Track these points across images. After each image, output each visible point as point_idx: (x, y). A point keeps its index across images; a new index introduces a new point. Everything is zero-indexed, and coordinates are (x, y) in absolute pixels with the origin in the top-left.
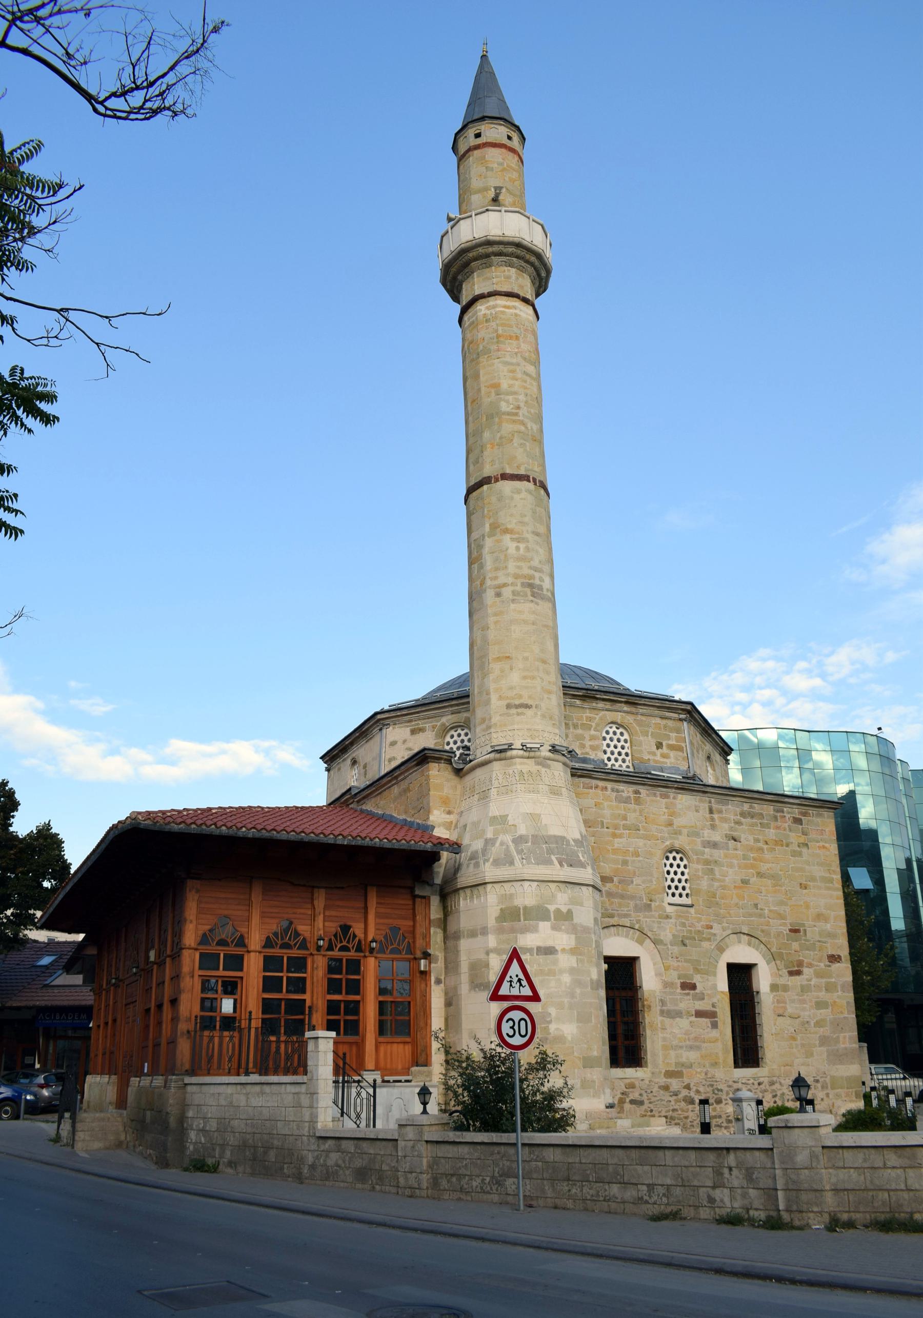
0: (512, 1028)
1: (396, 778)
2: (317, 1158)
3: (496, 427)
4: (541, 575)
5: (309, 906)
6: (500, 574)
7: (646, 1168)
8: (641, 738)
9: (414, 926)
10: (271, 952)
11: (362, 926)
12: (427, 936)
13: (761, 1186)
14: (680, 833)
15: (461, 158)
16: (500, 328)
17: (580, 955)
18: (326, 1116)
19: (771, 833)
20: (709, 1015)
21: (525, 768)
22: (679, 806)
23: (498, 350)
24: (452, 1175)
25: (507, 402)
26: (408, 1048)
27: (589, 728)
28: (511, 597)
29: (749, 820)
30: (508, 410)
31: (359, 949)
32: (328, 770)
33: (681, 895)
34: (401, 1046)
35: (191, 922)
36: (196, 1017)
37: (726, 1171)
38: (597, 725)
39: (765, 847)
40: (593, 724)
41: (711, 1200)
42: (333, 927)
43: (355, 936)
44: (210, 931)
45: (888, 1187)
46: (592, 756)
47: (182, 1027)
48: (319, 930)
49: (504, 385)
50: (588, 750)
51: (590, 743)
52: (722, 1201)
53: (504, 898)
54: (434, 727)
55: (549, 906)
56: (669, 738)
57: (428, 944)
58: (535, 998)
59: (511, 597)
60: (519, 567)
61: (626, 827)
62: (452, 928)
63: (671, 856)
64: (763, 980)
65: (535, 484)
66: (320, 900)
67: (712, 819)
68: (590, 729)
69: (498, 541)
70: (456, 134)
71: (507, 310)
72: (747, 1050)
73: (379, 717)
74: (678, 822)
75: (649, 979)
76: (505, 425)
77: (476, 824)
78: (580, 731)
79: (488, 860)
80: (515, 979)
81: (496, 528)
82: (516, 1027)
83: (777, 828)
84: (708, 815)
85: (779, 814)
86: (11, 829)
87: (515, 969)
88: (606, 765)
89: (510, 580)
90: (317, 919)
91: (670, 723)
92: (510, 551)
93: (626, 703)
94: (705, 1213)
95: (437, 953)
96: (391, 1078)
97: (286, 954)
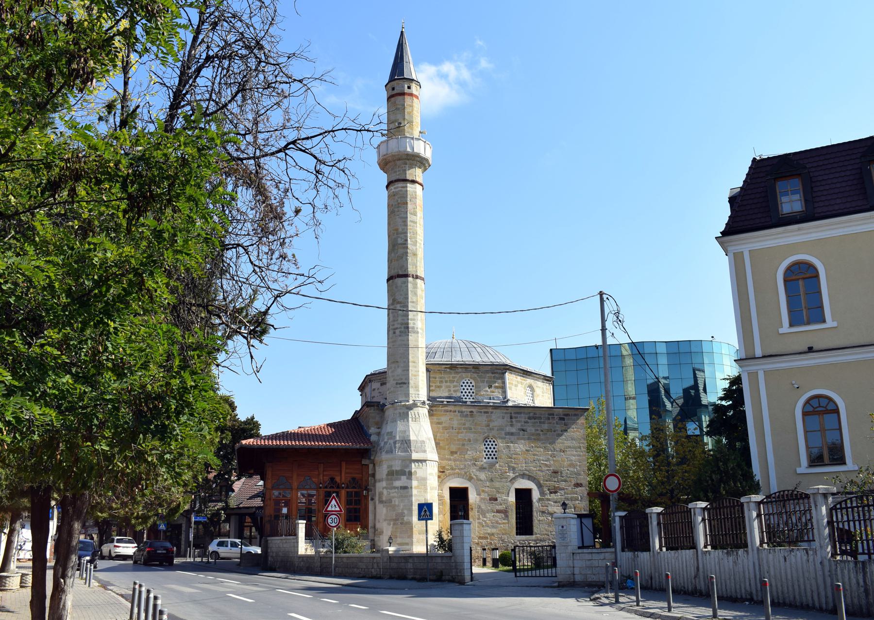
12: (367, 481)
20: (505, 512)
21: (401, 411)
49: (400, 230)
61: (464, 429)
64: (536, 495)
75: (473, 497)
91: (497, 375)
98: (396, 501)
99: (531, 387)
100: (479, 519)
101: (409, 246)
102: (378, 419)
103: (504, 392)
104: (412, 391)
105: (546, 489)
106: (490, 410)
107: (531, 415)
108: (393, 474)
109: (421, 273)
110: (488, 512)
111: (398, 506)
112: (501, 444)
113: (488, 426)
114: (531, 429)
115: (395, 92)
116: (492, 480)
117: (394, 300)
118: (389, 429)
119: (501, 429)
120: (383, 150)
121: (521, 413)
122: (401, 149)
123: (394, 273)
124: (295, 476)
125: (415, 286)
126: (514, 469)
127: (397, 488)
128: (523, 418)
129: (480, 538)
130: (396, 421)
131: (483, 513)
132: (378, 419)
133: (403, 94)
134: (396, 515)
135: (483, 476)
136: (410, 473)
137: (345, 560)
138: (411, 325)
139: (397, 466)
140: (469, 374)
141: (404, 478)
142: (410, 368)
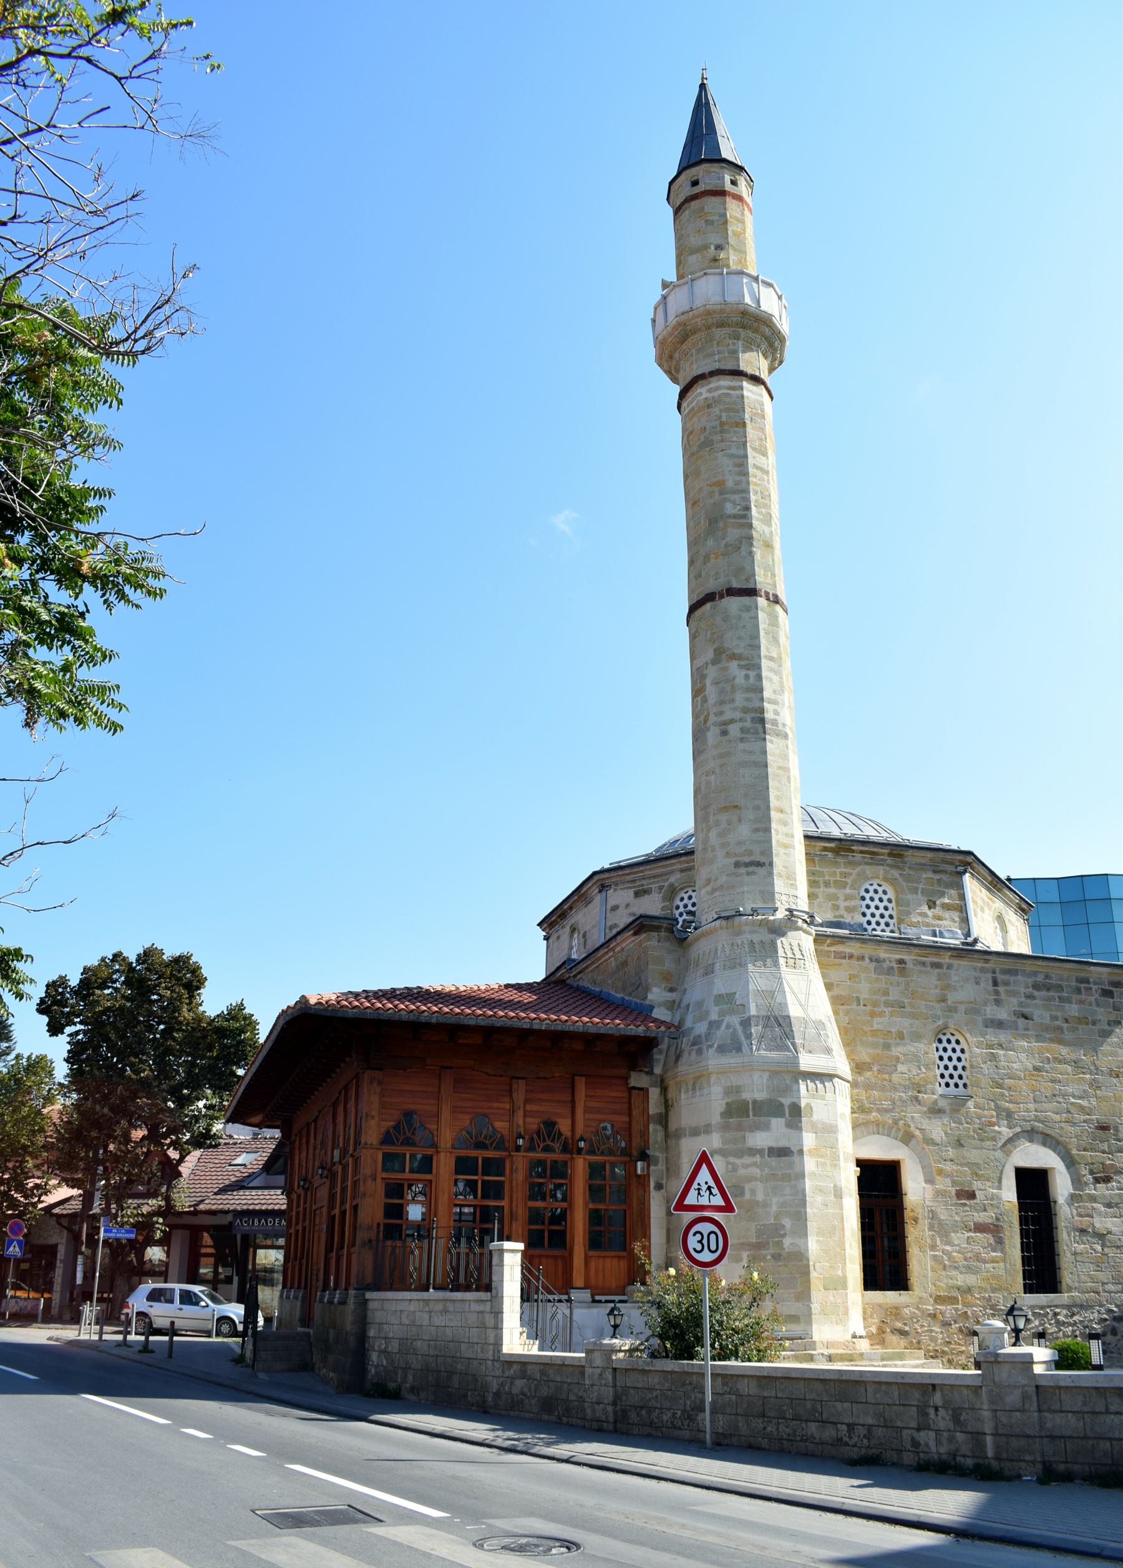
0: (700, 1242)
1: (613, 949)
2: (502, 1385)
3: (720, 533)
4: (775, 707)
5: (507, 1099)
6: (726, 707)
7: (847, 1405)
8: (910, 897)
9: (630, 1123)
10: (464, 1153)
11: (569, 1122)
12: (645, 1134)
13: (969, 1429)
14: (956, 1010)
15: (677, 212)
16: (724, 415)
17: (822, 1157)
18: (515, 1341)
19: (1073, 1010)
20: (994, 1229)
21: (756, 938)
22: (954, 978)
23: (722, 441)
24: (642, 1408)
25: (734, 503)
26: (624, 1264)
27: (844, 885)
28: (739, 735)
29: (1044, 993)
30: (734, 512)
31: (565, 1149)
32: (546, 938)
33: (956, 1085)
34: (615, 1261)
35: (373, 1117)
36: (379, 1224)
37: (932, 1411)
38: (854, 881)
39: (1065, 1025)
40: (849, 881)
41: (915, 1443)
42: (534, 1123)
43: (560, 1134)
44: (394, 1128)
45: (1110, 1435)
46: (848, 919)
47: (361, 1236)
48: (518, 1126)
49: (730, 484)
50: (842, 912)
51: (847, 904)
52: (927, 1445)
53: (728, 1091)
54: (661, 888)
55: (783, 1100)
56: (942, 894)
57: (647, 1145)
58: (728, 1208)
59: (739, 735)
60: (748, 699)
61: (887, 1004)
62: (673, 1126)
63: (944, 1038)
64: (1061, 1186)
65: (768, 599)
66: (520, 1091)
67: (997, 993)
68: (845, 887)
69: (725, 669)
70: (671, 183)
71: (732, 392)
72: (1041, 1271)
73: (596, 878)
74: (951, 998)
75: (915, 1188)
76: (729, 530)
77: (700, 1004)
78: (832, 890)
79: (711, 1046)
80: (704, 1187)
81: (721, 653)
82: (705, 1242)
83: (1081, 1002)
84: (991, 988)
85: (1083, 986)
86: (201, 1009)
87: (704, 1175)
88: (866, 930)
89: (738, 715)
90: (516, 1114)
91: (945, 877)
92: (737, 681)
93: (890, 855)
94: (908, 1458)
95: (657, 1154)
96: (603, 1298)
97: (481, 1154)
98: (758, 1191)
99: (1000, 918)
100: (933, 1247)
101: (755, 523)
102: (669, 965)
103: (965, 921)
104: (779, 885)
105: (1084, 1171)
106: (946, 959)
107: (1040, 978)
108: (741, 1113)
109: (782, 597)
110: (955, 1228)
111: (765, 1205)
112: (974, 1046)
113: (944, 1000)
114: (1041, 1015)
115: (701, 187)
116: (959, 1144)
117: (719, 653)
118: (721, 984)
119: (973, 1010)
120: (679, 302)
121: (1014, 972)
122: (730, 299)
123: (712, 585)
124: (446, 1114)
125: (774, 622)
126: (1009, 1115)
127: (760, 1152)
128: (1021, 984)
129: (939, 1299)
130: (743, 965)
131: (941, 1230)
132: (669, 965)
133: (722, 193)
134: (759, 1233)
135: (937, 1129)
136: (796, 1111)
137: (747, 1388)
138: (769, 715)
139: (756, 1089)
140: (881, 870)
141: (778, 1123)
142: (773, 825)
